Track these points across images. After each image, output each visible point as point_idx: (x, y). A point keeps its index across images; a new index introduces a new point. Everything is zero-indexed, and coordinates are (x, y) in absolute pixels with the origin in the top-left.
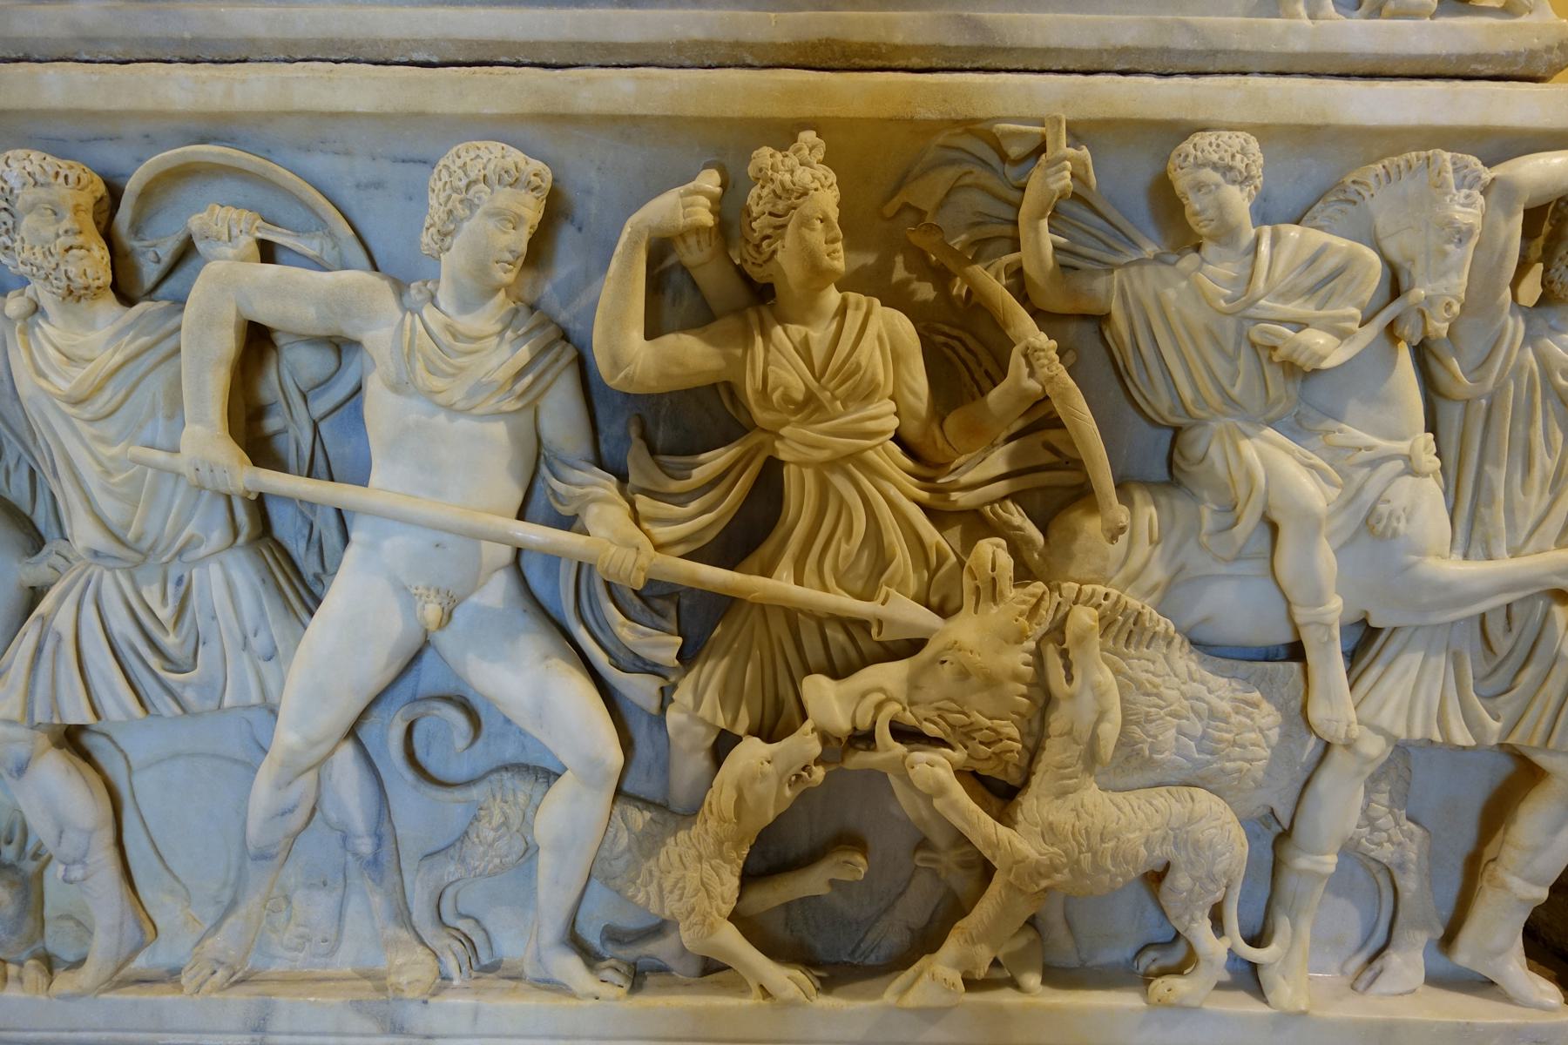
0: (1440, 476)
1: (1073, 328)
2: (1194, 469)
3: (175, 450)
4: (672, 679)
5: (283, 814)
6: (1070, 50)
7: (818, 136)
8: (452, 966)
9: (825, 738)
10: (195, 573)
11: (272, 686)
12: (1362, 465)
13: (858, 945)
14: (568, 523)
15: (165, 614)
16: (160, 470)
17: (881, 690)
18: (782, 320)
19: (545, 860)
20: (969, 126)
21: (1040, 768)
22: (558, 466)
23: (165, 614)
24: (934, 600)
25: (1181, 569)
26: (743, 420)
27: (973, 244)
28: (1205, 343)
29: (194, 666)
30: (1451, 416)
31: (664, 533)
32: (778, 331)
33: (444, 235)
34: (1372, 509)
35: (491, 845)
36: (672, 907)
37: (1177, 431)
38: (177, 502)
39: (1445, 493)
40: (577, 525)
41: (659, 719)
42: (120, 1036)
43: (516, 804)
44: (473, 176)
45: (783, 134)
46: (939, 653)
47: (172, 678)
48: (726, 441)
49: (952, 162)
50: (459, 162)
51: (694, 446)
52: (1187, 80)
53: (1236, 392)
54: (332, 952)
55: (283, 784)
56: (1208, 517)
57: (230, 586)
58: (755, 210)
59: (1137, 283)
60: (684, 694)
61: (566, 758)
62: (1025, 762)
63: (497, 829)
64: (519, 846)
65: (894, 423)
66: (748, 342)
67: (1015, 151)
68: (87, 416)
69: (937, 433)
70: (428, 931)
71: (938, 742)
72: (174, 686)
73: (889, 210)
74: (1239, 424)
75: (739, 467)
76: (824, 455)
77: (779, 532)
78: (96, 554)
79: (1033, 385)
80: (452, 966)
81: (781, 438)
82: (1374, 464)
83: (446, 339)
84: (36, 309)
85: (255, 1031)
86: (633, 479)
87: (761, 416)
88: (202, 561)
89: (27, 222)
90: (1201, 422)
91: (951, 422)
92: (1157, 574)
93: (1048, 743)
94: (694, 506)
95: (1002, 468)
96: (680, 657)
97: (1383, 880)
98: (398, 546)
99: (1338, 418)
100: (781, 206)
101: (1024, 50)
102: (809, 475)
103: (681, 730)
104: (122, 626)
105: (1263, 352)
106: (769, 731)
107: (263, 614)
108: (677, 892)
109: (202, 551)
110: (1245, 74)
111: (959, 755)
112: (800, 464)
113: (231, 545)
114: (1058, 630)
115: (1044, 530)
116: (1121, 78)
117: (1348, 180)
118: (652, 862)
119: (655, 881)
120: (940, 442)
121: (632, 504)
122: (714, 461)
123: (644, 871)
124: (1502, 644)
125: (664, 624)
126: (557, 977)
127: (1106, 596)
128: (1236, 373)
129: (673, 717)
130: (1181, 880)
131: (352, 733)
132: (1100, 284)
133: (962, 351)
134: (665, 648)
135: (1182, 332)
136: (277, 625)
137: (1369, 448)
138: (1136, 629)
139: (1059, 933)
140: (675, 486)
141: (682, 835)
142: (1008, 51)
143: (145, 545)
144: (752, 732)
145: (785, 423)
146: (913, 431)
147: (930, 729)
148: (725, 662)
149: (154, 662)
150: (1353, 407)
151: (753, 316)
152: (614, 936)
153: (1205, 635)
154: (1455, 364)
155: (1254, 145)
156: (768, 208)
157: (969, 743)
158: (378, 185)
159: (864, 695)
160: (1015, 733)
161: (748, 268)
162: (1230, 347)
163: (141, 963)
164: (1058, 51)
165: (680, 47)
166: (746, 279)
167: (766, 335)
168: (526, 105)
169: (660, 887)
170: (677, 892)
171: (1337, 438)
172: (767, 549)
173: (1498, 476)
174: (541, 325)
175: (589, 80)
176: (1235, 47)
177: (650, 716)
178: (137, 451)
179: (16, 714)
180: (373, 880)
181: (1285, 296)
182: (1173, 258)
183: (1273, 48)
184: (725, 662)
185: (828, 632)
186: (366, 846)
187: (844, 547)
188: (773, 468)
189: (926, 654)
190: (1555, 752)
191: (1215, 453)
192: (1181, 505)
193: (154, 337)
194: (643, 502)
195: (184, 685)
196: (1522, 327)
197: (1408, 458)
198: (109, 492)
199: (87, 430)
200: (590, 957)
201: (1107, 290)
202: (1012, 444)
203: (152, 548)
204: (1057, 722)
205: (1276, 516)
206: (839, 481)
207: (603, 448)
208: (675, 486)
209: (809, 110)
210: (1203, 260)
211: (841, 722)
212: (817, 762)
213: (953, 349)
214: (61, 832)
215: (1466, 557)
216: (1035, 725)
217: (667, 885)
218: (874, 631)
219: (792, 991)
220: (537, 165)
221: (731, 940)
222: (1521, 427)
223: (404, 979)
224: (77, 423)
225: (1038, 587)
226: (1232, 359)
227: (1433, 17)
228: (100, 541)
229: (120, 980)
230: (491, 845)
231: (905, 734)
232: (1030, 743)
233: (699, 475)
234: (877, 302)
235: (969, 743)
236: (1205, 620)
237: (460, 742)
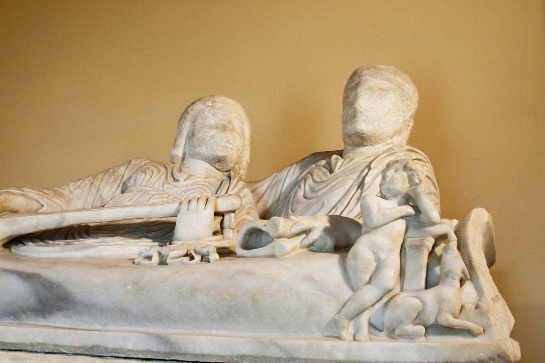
6: (215, 355)
101: (192, 355)
165: (32, 345)
176: (303, 356)
183: (326, 357)
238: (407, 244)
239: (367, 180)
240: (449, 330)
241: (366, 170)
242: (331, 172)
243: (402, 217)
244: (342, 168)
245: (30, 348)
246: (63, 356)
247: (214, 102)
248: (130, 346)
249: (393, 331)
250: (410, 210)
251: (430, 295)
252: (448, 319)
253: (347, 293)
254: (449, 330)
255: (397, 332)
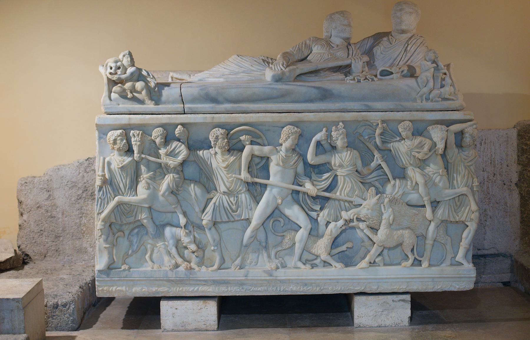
0: (447, 176)
1: (386, 152)
2: (406, 175)
3: (240, 174)
4: (319, 213)
5: (251, 238)
7: (343, 123)
8: (279, 265)
9: (346, 221)
10: (240, 195)
11: (250, 215)
12: (432, 174)
13: (351, 262)
14: (301, 186)
15: (234, 202)
16: (237, 178)
17: (354, 212)
18: (338, 153)
19: (297, 245)
20: (367, 121)
21: (381, 225)
22: (299, 176)
23: (234, 202)
24: (363, 198)
25: (404, 192)
26: (331, 168)
27: (368, 138)
28: (406, 155)
29: (237, 212)
30: (450, 165)
31: (318, 187)
32: (337, 155)
33: (284, 141)
34: (434, 181)
35: (287, 243)
36: (319, 252)
37: (404, 168)
38: (239, 184)
39: (448, 179)
40: (303, 186)
41: (317, 220)
42: (221, 278)
43: (292, 235)
44: (290, 132)
45: (336, 124)
46: (364, 206)
47: (232, 213)
48: (328, 172)
49: (365, 125)
50: (287, 130)
51: (321, 173)
52: (401, 112)
53: (411, 162)
54: (256, 265)
55: (253, 232)
56: (409, 183)
57: (246, 197)
58: (333, 136)
59: (395, 145)
60: (321, 214)
61: (302, 226)
62: (379, 225)
63: (288, 240)
64: (292, 243)
65: (356, 169)
66: (332, 156)
67: (374, 124)
68: (227, 170)
69: (363, 170)
70: (275, 260)
71: (364, 221)
72: (233, 215)
73: (355, 133)
74: (413, 168)
75: (330, 177)
76: (345, 174)
77: (337, 188)
78: (224, 192)
79: (378, 163)
80: (279, 265)
81: (338, 171)
82: (434, 174)
83: (285, 157)
84: (216, 153)
85: (246, 276)
86: (313, 178)
87: (334, 168)
88: (241, 194)
89: (220, 140)
90: (407, 167)
91: (365, 168)
92: (400, 192)
93: (382, 221)
94: (323, 183)
95: (375, 176)
96: (320, 209)
97: (444, 247)
98: (275, 191)
99: (429, 166)
100: (337, 136)
102: (342, 177)
103: (321, 221)
104: (226, 204)
105: (414, 156)
106: (336, 220)
107: (251, 201)
108: (320, 250)
109: (242, 191)
110: (411, 111)
111: (368, 223)
112: (341, 176)
113: (246, 191)
114: (383, 203)
115: (382, 187)
116: (391, 113)
117: (428, 128)
118: (316, 245)
119: (316, 248)
120: (364, 172)
121: (313, 183)
122: (326, 175)
123: (314, 246)
124: (458, 204)
125: (317, 203)
126: (298, 267)
127: (391, 196)
128: (411, 160)
129: (319, 219)
130: (405, 244)
131: (263, 224)
132: (389, 145)
133: (367, 156)
134: (318, 208)
135: (402, 153)
136: (253, 205)
137: (433, 171)
138: (397, 202)
139: (387, 258)
140: (320, 180)
141: (321, 239)
142: (372, 109)
143: (232, 191)
144: (332, 221)
145: (338, 169)
146: (359, 169)
147: (363, 219)
148: (328, 209)
149: (230, 211)
150: (432, 165)
151: (333, 152)
152: (307, 261)
153: (409, 203)
154: (448, 157)
155: (411, 124)
156: (336, 136)
157: (370, 221)
158: (269, 130)
159: (352, 213)
160: (375, 218)
161: (332, 144)
162: (410, 156)
163: (222, 267)
164: (381, 109)
165: (320, 110)
166: (331, 145)
167: (335, 156)
168: (296, 120)
169: (317, 249)
170: (320, 250)
171: (428, 170)
172: (336, 189)
173: (455, 175)
174: (298, 154)
175: (306, 116)
177: (315, 219)
178: (233, 176)
179: (211, 219)
180: (265, 250)
181: (418, 148)
182: (401, 141)
184: (328, 209)
185: (346, 204)
186: (264, 244)
187: (348, 189)
188: (336, 176)
189: (362, 206)
190: (467, 221)
191: (409, 172)
192: (404, 182)
193: (237, 156)
194: (315, 183)
195: (235, 215)
196: (457, 151)
197: (439, 173)
198: (227, 181)
199: (225, 172)
200: (304, 264)
201: (390, 146)
202: (376, 172)
203: (233, 192)
204: (384, 217)
205: (418, 183)
206: (347, 179)
207: (306, 173)
208: (320, 180)
209: (341, 119)
210: (405, 142)
211: (347, 218)
212: (345, 224)
213: (366, 156)
214: (214, 241)
215: (452, 189)
216: (380, 218)
217: (319, 248)
218: (353, 203)
219: (340, 267)
220: (299, 130)
221: (329, 257)
222: (458, 168)
223: (272, 267)
224: (223, 171)
225: (379, 195)
226: (410, 157)
227: (441, 101)
228: (226, 190)
229: (219, 269)
230: (287, 243)
231: (359, 220)
232: (380, 221)
233: (324, 178)
234: (353, 149)
235: (370, 221)
236: (409, 201)
237: (282, 225)
238: (434, 75)
239: (408, 49)
240: (447, 99)
241: (407, 45)
242: (391, 44)
243: (433, 67)
244: (396, 43)
245: (319, 111)
246: (331, 113)
247: (343, 14)
248: (355, 108)
249: (432, 100)
250: (436, 65)
251: (442, 90)
252: (447, 96)
253: (419, 89)
254: (447, 99)
255: (433, 100)
